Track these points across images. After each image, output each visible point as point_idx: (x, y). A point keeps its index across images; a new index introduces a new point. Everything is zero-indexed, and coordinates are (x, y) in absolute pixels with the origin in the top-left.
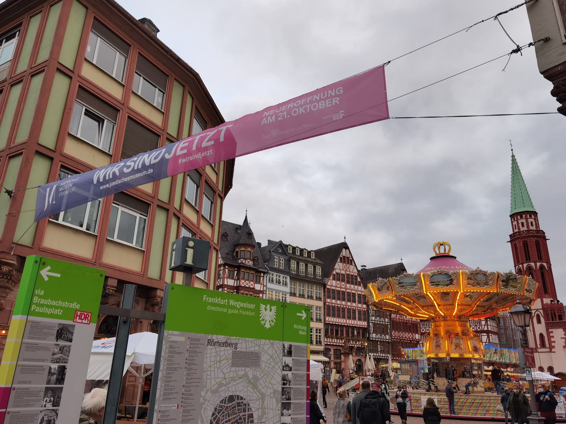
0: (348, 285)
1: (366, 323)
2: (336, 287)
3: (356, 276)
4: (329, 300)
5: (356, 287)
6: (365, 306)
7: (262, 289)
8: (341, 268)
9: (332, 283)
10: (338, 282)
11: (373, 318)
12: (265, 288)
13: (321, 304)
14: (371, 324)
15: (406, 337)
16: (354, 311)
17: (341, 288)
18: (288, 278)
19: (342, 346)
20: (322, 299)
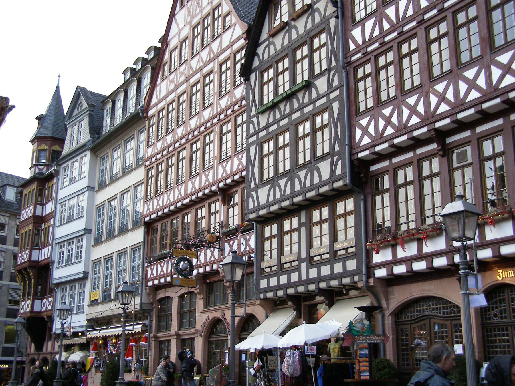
7: (53, 210)
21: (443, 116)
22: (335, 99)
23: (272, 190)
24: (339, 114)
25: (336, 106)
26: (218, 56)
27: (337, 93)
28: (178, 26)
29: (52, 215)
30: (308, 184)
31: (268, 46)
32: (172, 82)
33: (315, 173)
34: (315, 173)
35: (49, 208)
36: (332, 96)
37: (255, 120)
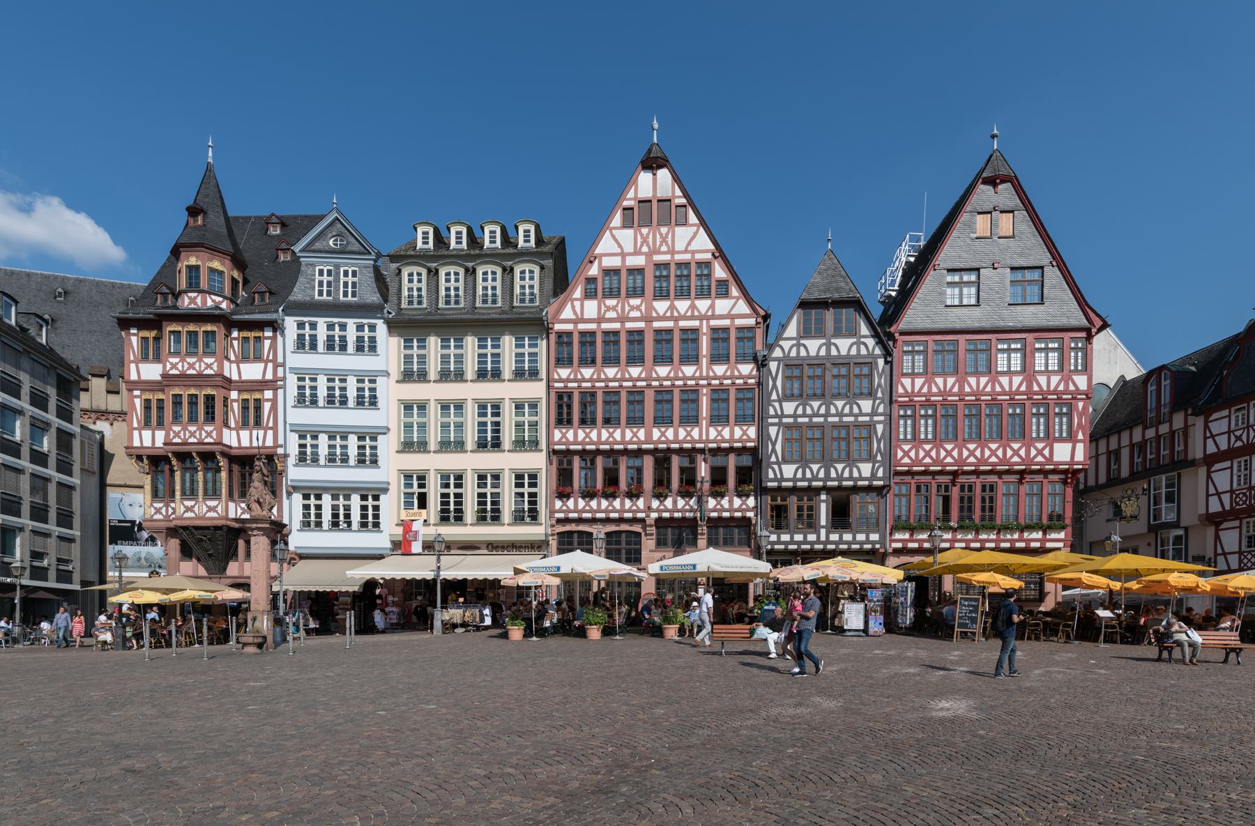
0: (661, 306)
1: (752, 432)
2: (600, 320)
3: (707, 264)
4: (564, 373)
5: (703, 305)
6: (747, 369)
7: (269, 376)
8: (629, 248)
9: (579, 312)
10: (611, 302)
11: (789, 407)
12: (280, 370)
13: (535, 390)
14: (773, 431)
15: (982, 461)
16: (690, 395)
17: (622, 319)
18: (381, 327)
19: (634, 520)
20: (543, 374)
21: (970, 464)
22: (879, 422)
23: (800, 471)
24: (883, 434)
25: (880, 428)
26: (708, 318)
27: (882, 418)
28: (620, 246)
29: (272, 384)
30: (846, 474)
31: (798, 345)
32: (608, 309)
33: (855, 470)
34: (855, 470)
35: (252, 371)
36: (876, 418)
37: (777, 405)
